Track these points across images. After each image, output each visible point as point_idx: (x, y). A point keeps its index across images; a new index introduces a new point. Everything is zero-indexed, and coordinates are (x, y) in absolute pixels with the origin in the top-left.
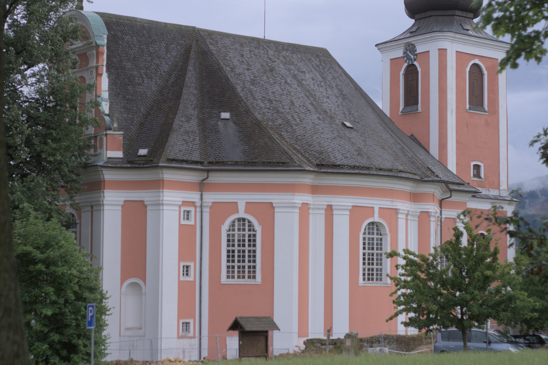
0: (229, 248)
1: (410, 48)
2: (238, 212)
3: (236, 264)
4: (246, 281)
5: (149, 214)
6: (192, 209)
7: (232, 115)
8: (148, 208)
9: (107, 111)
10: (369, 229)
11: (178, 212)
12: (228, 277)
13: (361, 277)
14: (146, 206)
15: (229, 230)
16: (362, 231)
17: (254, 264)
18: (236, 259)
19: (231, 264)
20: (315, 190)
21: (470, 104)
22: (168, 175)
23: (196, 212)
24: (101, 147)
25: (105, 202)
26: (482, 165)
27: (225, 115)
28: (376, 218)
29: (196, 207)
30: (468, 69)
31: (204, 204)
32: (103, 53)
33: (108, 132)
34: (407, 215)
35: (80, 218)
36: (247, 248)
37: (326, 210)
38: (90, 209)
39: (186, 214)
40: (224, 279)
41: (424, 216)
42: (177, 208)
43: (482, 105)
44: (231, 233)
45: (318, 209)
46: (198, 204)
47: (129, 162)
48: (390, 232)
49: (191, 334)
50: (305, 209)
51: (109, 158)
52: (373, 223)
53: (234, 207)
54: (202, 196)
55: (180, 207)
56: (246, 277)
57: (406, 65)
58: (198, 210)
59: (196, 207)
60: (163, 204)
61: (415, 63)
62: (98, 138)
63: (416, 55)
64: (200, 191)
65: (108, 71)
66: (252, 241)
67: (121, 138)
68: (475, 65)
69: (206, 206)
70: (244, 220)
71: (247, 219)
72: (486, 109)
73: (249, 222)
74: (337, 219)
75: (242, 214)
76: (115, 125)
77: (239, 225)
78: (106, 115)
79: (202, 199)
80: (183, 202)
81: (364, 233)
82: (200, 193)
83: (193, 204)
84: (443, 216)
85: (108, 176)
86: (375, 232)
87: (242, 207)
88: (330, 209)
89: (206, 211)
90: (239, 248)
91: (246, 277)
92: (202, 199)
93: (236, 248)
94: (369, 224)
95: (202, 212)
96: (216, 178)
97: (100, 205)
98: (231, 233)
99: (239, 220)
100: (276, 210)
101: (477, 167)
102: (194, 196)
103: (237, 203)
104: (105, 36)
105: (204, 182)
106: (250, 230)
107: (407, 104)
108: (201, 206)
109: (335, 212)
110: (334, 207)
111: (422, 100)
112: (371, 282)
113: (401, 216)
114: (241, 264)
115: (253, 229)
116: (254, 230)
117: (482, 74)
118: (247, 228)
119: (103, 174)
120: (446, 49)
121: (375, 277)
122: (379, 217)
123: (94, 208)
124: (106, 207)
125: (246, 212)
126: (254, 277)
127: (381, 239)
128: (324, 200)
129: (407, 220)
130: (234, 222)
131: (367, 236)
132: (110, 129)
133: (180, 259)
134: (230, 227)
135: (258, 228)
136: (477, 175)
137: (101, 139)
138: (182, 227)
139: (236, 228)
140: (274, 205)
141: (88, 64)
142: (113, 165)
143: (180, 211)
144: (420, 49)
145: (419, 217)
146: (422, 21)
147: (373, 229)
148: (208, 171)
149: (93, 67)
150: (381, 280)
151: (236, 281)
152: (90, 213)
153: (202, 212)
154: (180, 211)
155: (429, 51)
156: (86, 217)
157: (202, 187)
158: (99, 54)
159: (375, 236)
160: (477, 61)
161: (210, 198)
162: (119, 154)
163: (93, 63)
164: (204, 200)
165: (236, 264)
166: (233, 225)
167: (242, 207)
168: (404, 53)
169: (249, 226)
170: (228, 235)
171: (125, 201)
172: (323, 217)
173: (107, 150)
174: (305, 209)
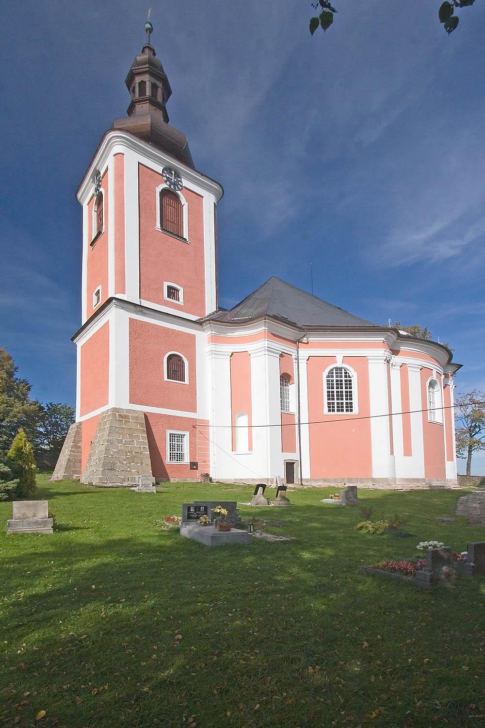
2: (336, 362)
12: (329, 411)
15: (328, 377)
44: (330, 379)
56: (345, 410)
66: (349, 383)
70: (341, 369)
71: (344, 368)
75: (339, 364)
87: (339, 359)
91: (345, 410)
99: (337, 369)
106: (346, 377)
116: (349, 377)
126: (351, 411)
167: (339, 359)
169: (346, 373)
170: (328, 381)
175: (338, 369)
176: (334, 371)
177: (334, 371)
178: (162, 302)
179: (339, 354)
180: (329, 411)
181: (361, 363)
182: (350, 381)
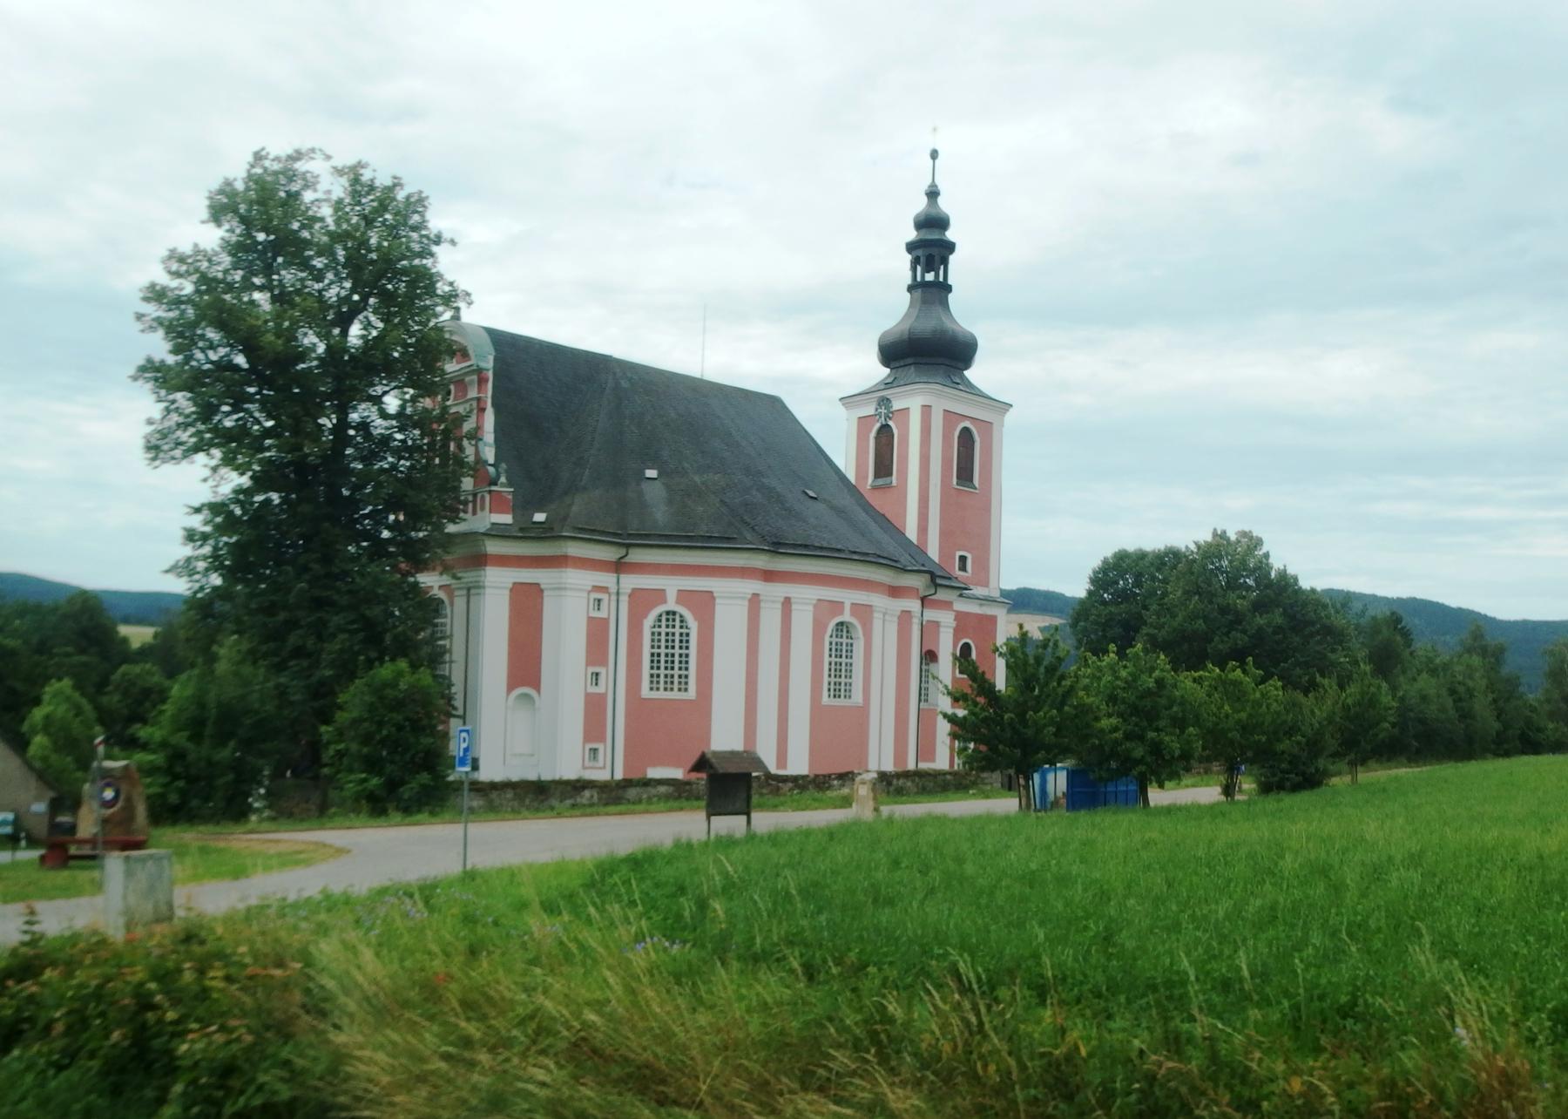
0: (653, 651)
1: (884, 402)
3: (662, 672)
4: (675, 695)
5: (546, 600)
6: (604, 597)
7: (659, 474)
8: (546, 593)
9: (491, 461)
10: (837, 630)
11: (586, 601)
12: (651, 689)
13: (825, 693)
14: (542, 591)
15: (654, 627)
16: (829, 632)
17: (686, 673)
18: (662, 665)
19: (655, 672)
20: (769, 576)
21: (958, 478)
22: (574, 549)
23: (609, 600)
24: (483, 509)
25: (487, 584)
26: (969, 556)
27: (651, 473)
28: (846, 617)
29: (610, 594)
30: (957, 433)
32: (487, 381)
33: (494, 488)
34: (884, 614)
35: (452, 604)
36: (677, 651)
37: (783, 604)
38: (465, 592)
39: (596, 603)
40: (645, 692)
41: (905, 616)
42: (585, 595)
43: (971, 479)
44: (657, 630)
45: (773, 602)
46: (613, 590)
47: (521, 530)
48: (864, 635)
49: (601, 764)
50: (755, 601)
51: (493, 524)
52: (842, 624)
53: (660, 595)
55: (589, 592)
57: (878, 425)
58: (614, 598)
59: (610, 594)
60: (565, 589)
61: (891, 423)
62: (479, 496)
63: (892, 413)
65: (494, 405)
66: (685, 640)
67: (510, 497)
68: (966, 431)
70: (674, 613)
72: (977, 485)
73: (681, 616)
74: (795, 616)
75: (671, 605)
76: (503, 479)
77: (668, 620)
78: (490, 465)
80: (594, 587)
81: (831, 636)
83: (604, 589)
84: (925, 618)
85: (493, 547)
86: (845, 634)
88: (787, 602)
89: (624, 600)
90: (667, 651)
93: (663, 651)
94: (837, 625)
95: (618, 601)
96: (637, 556)
97: (479, 587)
98: (657, 630)
99: (668, 613)
100: (718, 601)
101: (963, 559)
102: (607, 579)
103: (664, 590)
104: (491, 358)
105: (623, 561)
106: (681, 627)
107: (877, 475)
108: (618, 594)
109: (794, 607)
110: (793, 600)
111: (897, 471)
112: (837, 699)
113: (877, 616)
114: (669, 672)
116: (687, 628)
117: (973, 442)
118: (677, 623)
119: (484, 545)
120: (930, 406)
121: (842, 693)
122: (853, 614)
123: (472, 591)
124: (488, 591)
125: (678, 602)
126: (686, 690)
127: (852, 645)
128: (780, 590)
129: (884, 621)
130: (661, 616)
131: (834, 640)
132: (496, 484)
133: (589, 663)
135: (693, 625)
136: (963, 568)
137: (483, 498)
138: (590, 619)
139: (664, 623)
140: (715, 595)
141: (466, 395)
142: (498, 533)
143: (588, 599)
144: (897, 405)
145: (899, 618)
146: (900, 370)
147: (842, 631)
148: (628, 546)
149: (472, 399)
150: (850, 697)
151: (661, 694)
152: (465, 599)
153: (618, 601)
154: (588, 599)
155: (908, 409)
156: (460, 603)
157: (619, 567)
158: (482, 381)
159: (844, 640)
160: (967, 424)
161: (630, 582)
162: (507, 519)
163: (473, 393)
164: (621, 585)
165: (662, 672)
166: (660, 621)
168: (877, 410)
169: (682, 621)
171: (515, 583)
172: (779, 613)
173: (490, 512)
174: (755, 601)
175: (671, 613)
179: (672, 585)
180: (651, 689)
181: (704, 604)
182: (688, 635)
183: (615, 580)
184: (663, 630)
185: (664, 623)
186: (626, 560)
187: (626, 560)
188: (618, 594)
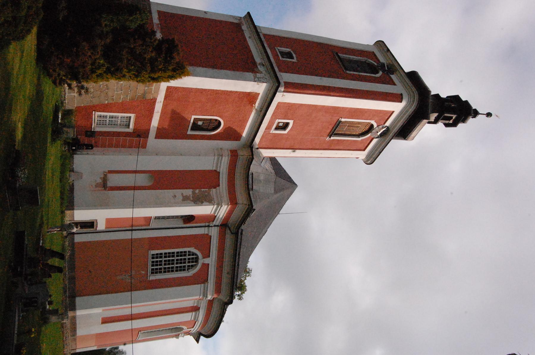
4: (150, 268)
15: (189, 252)
31: (210, 228)
54: (217, 226)
64: (221, 225)
69: (208, 231)
77: (193, 258)
79: (215, 226)
82: (219, 225)
92: (215, 226)
106: (189, 266)
115: (189, 269)
125: (204, 264)
134: (192, 252)
139: (191, 257)
151: (150, 260)
169: (192, 266)
175: (196, 260)
176: (194, 257)
177: (194, 257)
178: (275, 116)
183: (217, 224)
184: (187, 257)
185: (191, 257)
186: (227, 229)
187: (227, 229)
188: (209, 226)
